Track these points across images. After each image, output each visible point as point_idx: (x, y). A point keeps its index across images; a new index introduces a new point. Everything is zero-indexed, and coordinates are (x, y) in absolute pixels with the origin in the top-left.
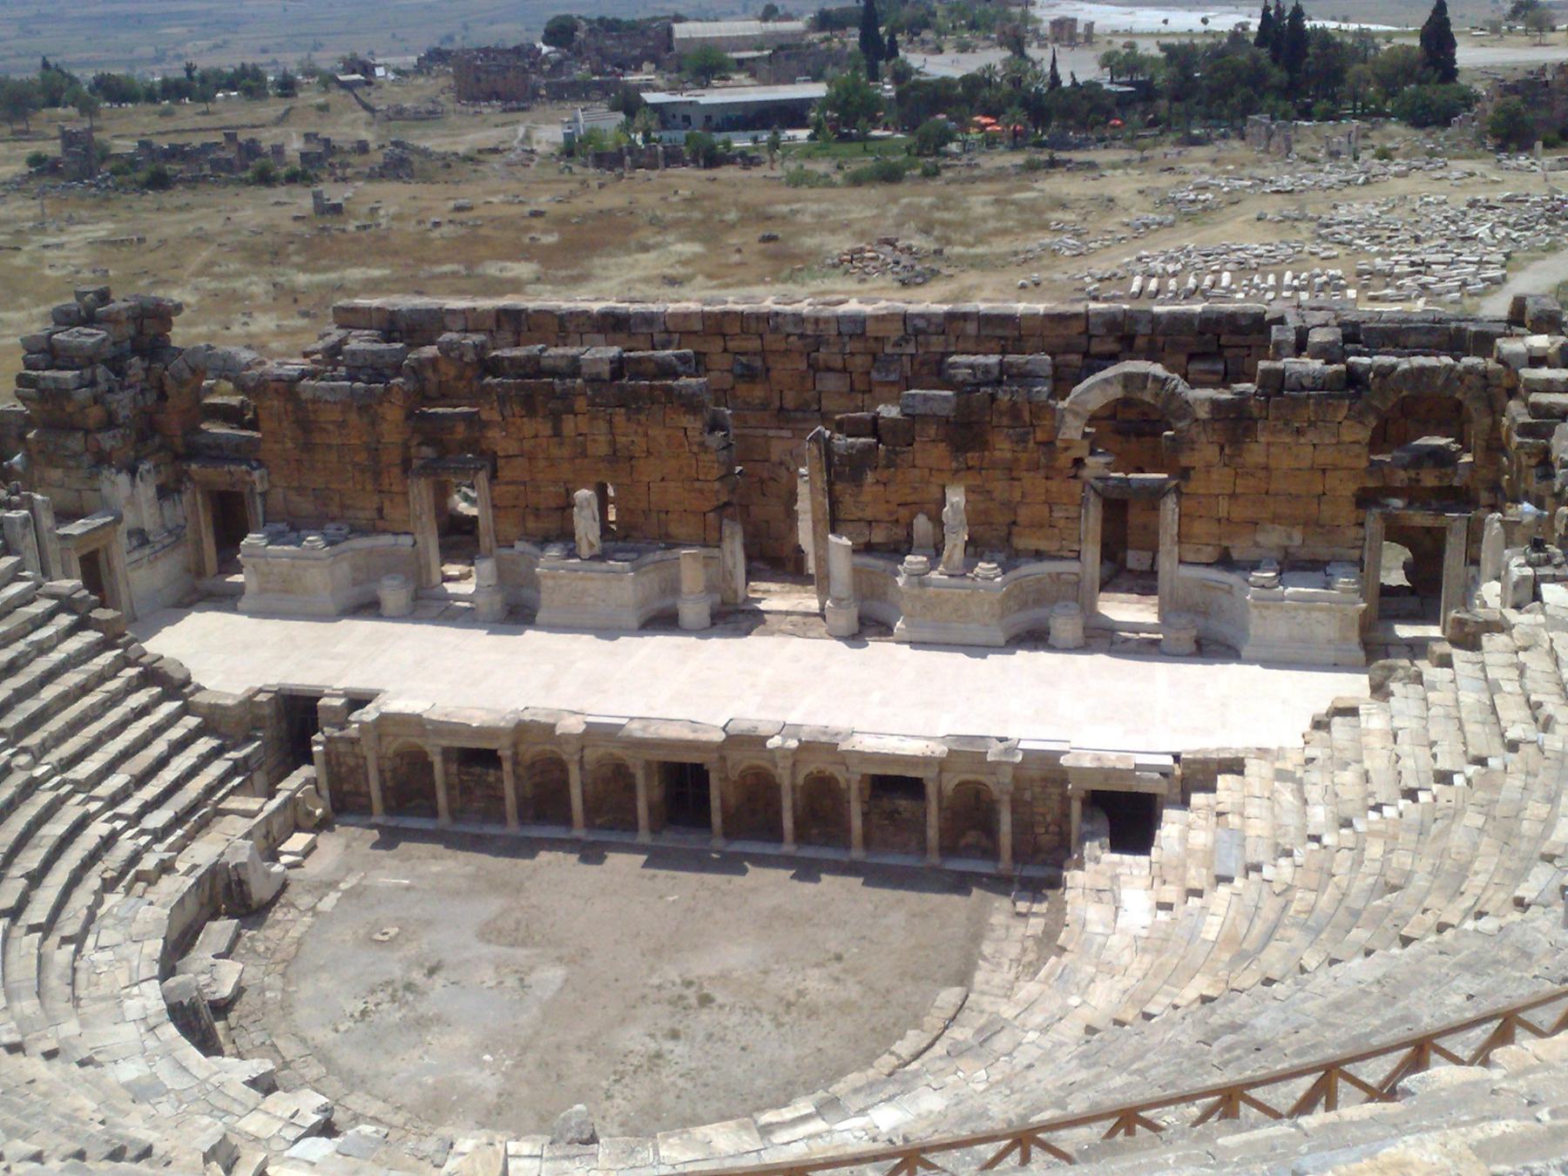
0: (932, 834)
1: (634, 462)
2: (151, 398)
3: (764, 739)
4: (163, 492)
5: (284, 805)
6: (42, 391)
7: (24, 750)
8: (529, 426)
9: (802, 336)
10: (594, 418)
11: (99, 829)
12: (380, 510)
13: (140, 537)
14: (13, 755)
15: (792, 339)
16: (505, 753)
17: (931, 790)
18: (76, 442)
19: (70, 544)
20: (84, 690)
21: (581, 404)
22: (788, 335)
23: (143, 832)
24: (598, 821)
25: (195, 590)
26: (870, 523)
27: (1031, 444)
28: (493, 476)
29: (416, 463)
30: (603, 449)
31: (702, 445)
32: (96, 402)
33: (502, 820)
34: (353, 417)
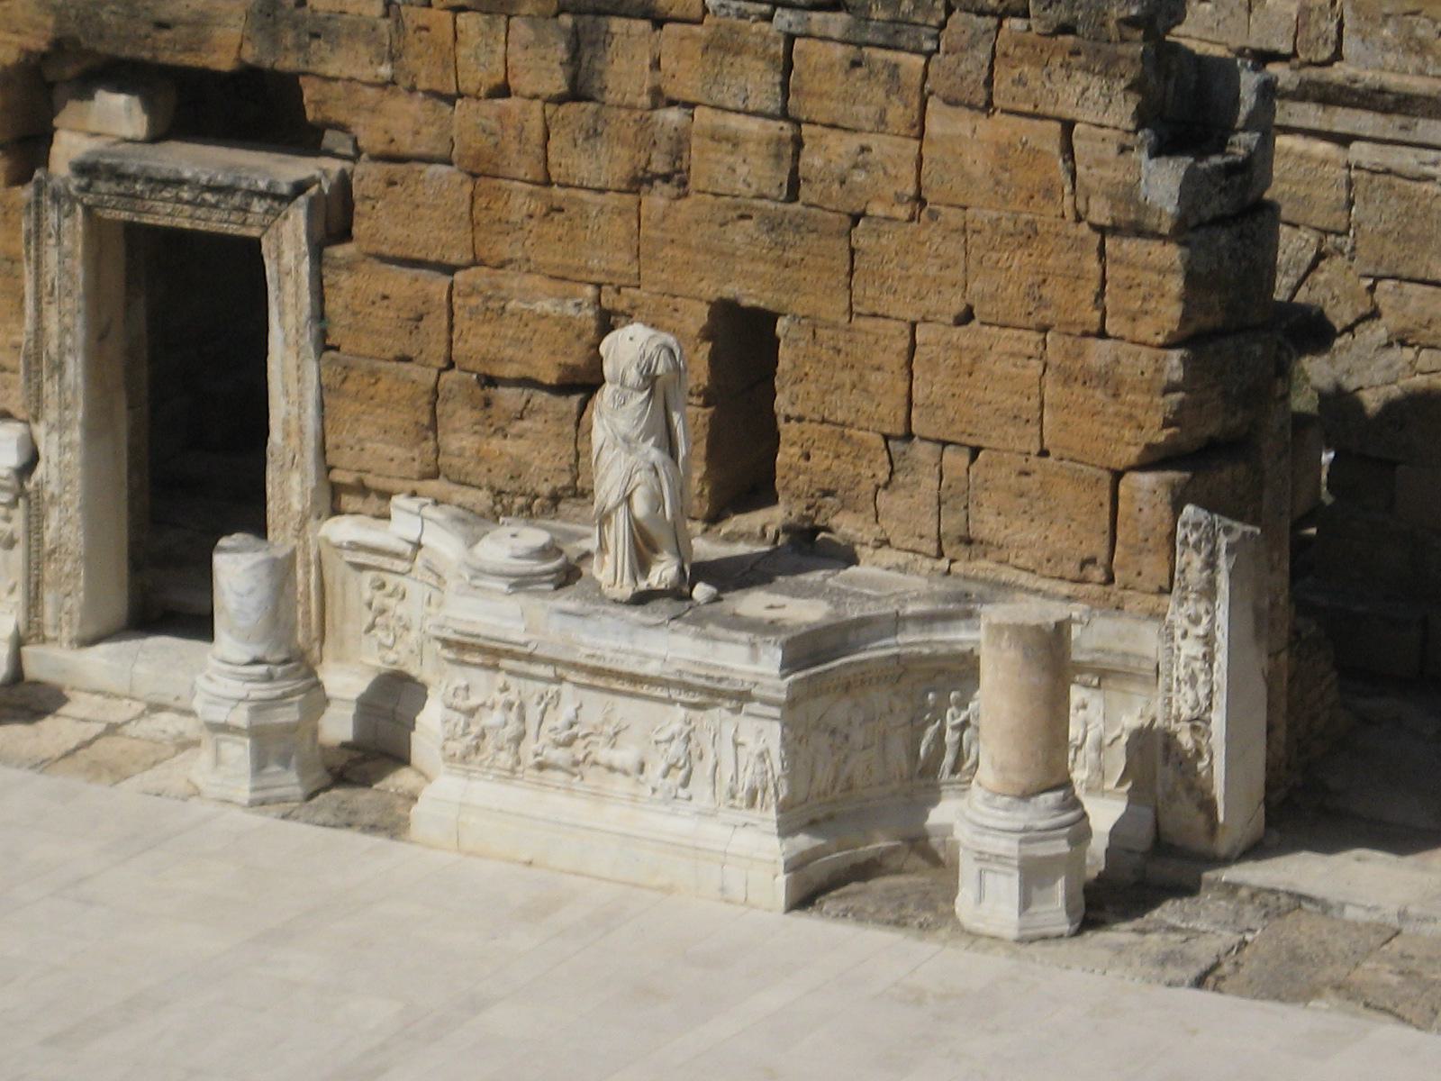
1: (862, 237)
28: (334, 221)
30: (753, 172)
31: (1128, 195)
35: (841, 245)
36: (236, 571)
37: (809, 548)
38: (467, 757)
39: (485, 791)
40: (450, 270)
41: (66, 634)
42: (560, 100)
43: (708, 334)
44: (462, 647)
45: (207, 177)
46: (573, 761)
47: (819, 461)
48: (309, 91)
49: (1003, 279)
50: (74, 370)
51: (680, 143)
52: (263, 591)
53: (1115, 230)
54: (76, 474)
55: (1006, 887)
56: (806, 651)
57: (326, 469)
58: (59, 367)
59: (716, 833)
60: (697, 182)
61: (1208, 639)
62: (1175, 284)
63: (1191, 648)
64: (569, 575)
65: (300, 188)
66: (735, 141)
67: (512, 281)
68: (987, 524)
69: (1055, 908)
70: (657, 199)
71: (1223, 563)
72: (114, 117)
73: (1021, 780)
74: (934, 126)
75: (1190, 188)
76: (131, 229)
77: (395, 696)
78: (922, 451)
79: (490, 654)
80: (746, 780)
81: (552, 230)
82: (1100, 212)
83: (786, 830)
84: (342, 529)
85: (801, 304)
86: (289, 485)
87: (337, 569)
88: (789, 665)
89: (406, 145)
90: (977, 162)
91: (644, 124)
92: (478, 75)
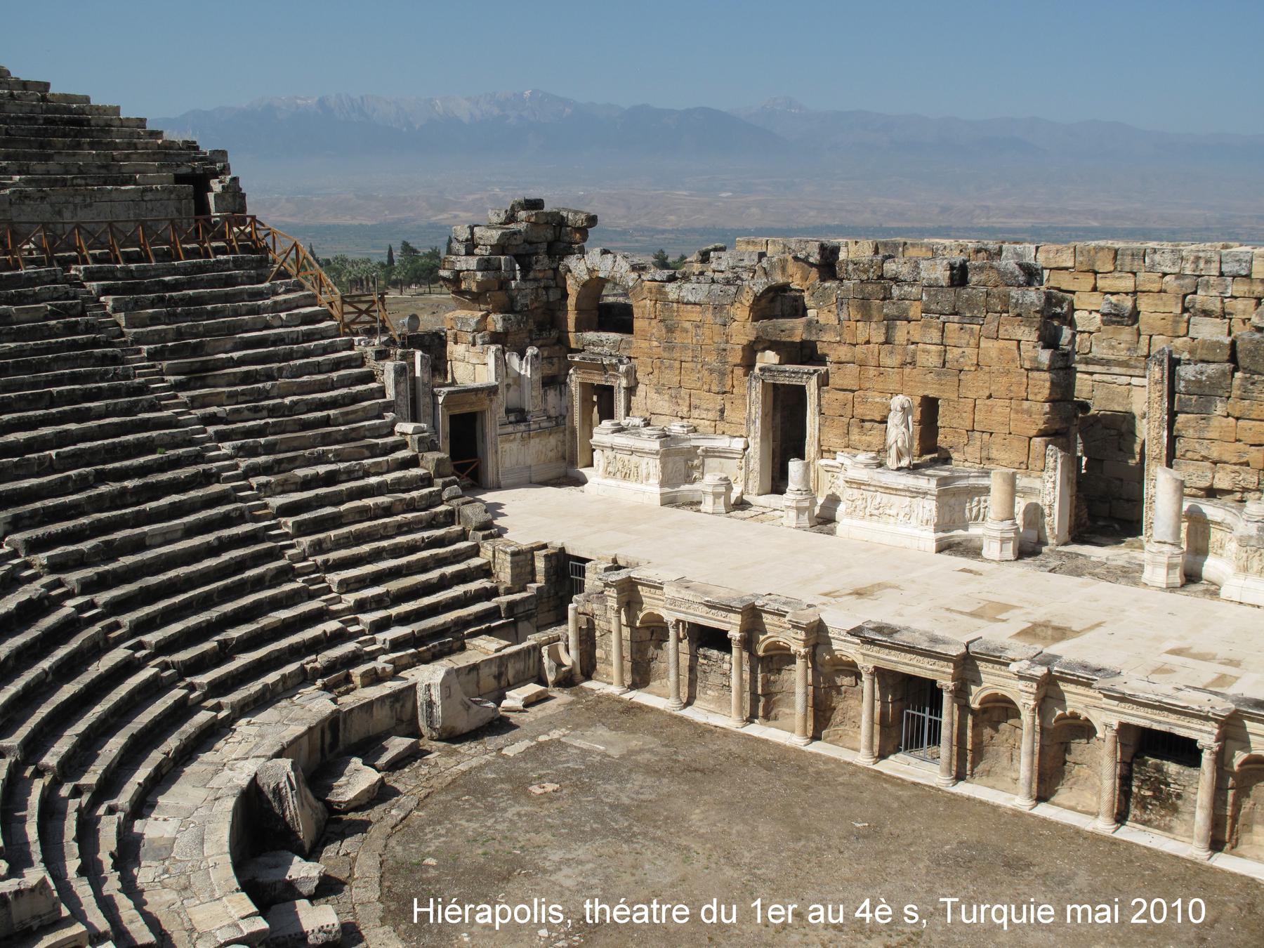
1: (962, 377)
5: (528, 651)
8: (863, 331)
9: (1179, 276)
10: (927, 326)
11: (332, 626)
12: (722, 411)
15: (1167, 278)
16: (735, 634)
20: (387, 511)
21: (915, 310)
22: (1165, 274)
25: (566, 476)
26: (1215, 463)
28: (824, 381)
30: (934, 361)
31: (1035, 359)
32: (500, 288)
34: (709, 316)
35: (956, 379)
36: (794, 466)
37: (946, 460)
38: (850, 514)
39: (856, 522)
40: (853, 391)
41: (756, 491)
42: (883, 344)
43: (920, 405)
44: (850, 482)
45: (794, 374)
46: (878, 514)
47: (949, 438)
48: (819, 345)
49: (1000, 386)
50: (758, 422)
51: (914, 354)
52: (801, 471)
53: (1031, 370)
54: (758, 450)
55: (996, 546)
56: (943, 481)
57: (820, 445)
58: (754, 422)
59: (917, 532)
60: (918, 364)
61: (1054, 482)
62: (1048, 384)
63: (1050, 485)
64: (880, 465)
65: (815, 371)
66: (928, 352)
67: (869, 394)
68: (994, 454)
69: (1009, 552)
70: (907, 370)
71: (1059, 461)
72: (769, 358)
73: (1002, 516)
74: (982, 345)
75: (1052, 360)
76: (774, 385)
77: (834, 500)
78: (977, 434)
79: (859, 485)
80: (926, 517)
81: (882, 378)
82: (1027, 365)
83: (936, 531)
84: (823, 462)
85: (945, 396)
86: (811, 448)
87: (822, 472)
88: (938, 485)
89: (843, 359)
90: (994, 354)
91: (905, 349)
92: (861, 339)
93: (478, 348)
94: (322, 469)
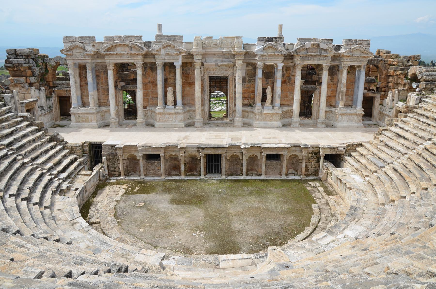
0: (284, 170)
2: (44, 71)
3: (239, 147)
4: (47, 97)
6: (13, 64)
7: (20, 155)
13: (41, 107)
14: (17, 156)
16: (162, 154)
17: (285, 157)
18: (23, 79)
19: (24, 105)
23: (60, 179)
24: (187, 174)
27: (285, 77)
29: (119, 87)
33: (160, 175)
93: (26, 88)
94: (9, 130)
